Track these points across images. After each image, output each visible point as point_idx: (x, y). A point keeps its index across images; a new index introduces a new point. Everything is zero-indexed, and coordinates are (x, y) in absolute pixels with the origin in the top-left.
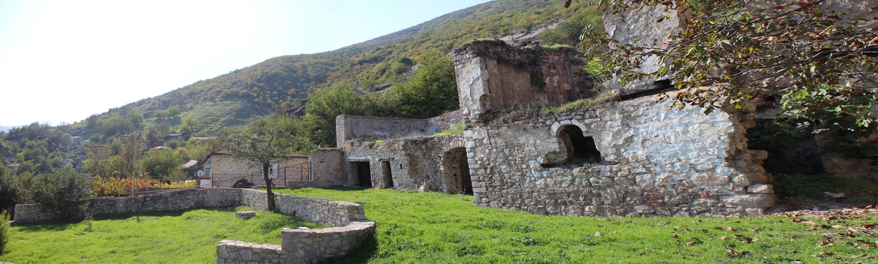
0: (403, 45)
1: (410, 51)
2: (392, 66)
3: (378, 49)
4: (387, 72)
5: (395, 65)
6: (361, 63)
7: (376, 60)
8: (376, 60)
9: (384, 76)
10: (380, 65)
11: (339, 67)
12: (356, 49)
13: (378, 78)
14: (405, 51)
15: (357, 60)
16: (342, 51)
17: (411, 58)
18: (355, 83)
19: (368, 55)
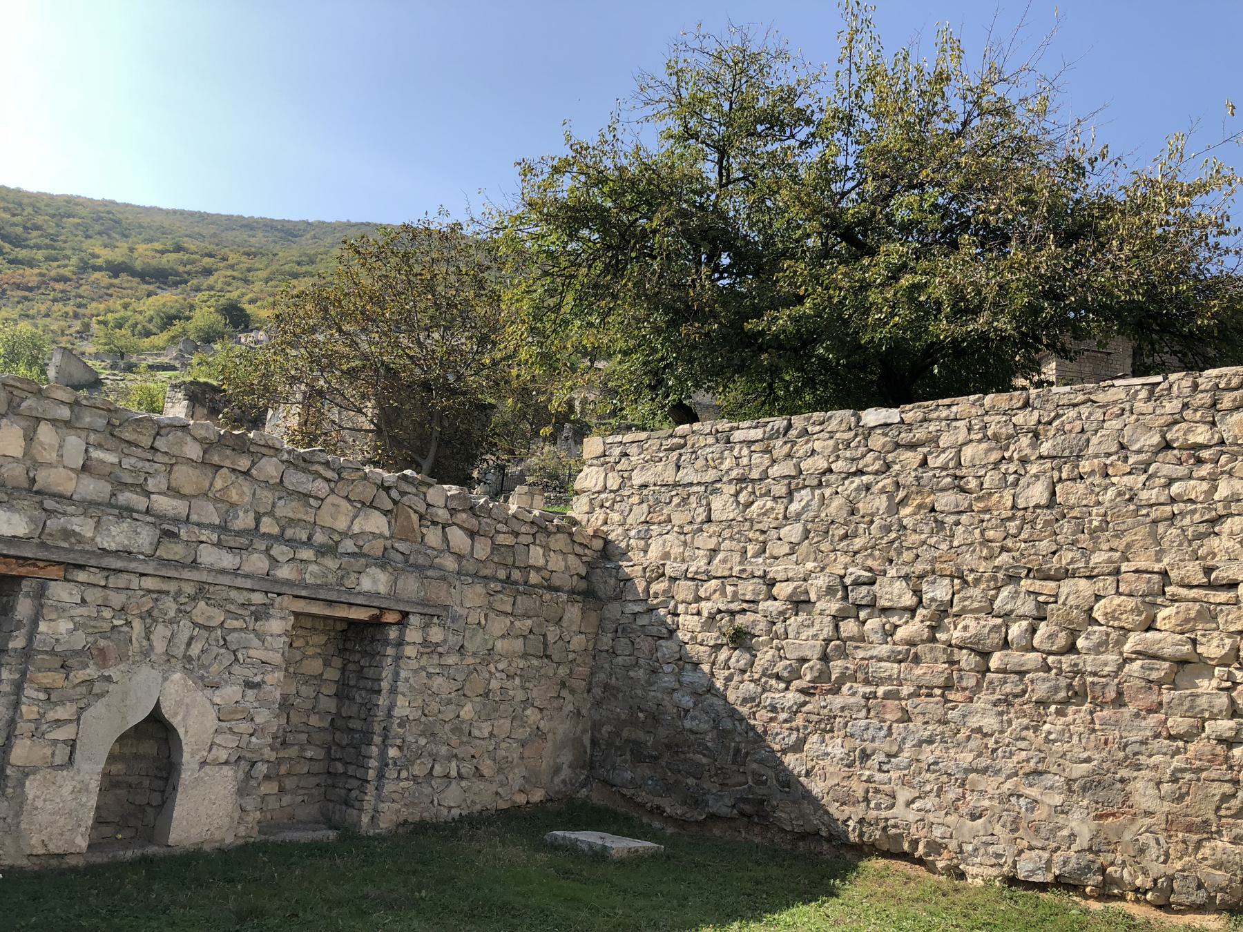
0: (246, 262)
1: (258, 286)
2: (197, 314)
3: (178, 249)
4: (178, 327)
5: (205, 316)
6: (115, 270)
7: (160, 277)
8: (160, 277)
9: (165, 336)
10: (168, 299)
11: (40, 255)
12: (110, 220)
13: (148, 334)
14: (246, 281)
15: (105, 255)
16: (65, 209)
17: (250, 309)
18: (77, 325)
19: (144, 254)
